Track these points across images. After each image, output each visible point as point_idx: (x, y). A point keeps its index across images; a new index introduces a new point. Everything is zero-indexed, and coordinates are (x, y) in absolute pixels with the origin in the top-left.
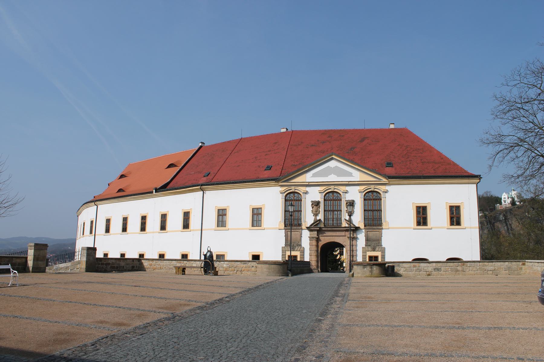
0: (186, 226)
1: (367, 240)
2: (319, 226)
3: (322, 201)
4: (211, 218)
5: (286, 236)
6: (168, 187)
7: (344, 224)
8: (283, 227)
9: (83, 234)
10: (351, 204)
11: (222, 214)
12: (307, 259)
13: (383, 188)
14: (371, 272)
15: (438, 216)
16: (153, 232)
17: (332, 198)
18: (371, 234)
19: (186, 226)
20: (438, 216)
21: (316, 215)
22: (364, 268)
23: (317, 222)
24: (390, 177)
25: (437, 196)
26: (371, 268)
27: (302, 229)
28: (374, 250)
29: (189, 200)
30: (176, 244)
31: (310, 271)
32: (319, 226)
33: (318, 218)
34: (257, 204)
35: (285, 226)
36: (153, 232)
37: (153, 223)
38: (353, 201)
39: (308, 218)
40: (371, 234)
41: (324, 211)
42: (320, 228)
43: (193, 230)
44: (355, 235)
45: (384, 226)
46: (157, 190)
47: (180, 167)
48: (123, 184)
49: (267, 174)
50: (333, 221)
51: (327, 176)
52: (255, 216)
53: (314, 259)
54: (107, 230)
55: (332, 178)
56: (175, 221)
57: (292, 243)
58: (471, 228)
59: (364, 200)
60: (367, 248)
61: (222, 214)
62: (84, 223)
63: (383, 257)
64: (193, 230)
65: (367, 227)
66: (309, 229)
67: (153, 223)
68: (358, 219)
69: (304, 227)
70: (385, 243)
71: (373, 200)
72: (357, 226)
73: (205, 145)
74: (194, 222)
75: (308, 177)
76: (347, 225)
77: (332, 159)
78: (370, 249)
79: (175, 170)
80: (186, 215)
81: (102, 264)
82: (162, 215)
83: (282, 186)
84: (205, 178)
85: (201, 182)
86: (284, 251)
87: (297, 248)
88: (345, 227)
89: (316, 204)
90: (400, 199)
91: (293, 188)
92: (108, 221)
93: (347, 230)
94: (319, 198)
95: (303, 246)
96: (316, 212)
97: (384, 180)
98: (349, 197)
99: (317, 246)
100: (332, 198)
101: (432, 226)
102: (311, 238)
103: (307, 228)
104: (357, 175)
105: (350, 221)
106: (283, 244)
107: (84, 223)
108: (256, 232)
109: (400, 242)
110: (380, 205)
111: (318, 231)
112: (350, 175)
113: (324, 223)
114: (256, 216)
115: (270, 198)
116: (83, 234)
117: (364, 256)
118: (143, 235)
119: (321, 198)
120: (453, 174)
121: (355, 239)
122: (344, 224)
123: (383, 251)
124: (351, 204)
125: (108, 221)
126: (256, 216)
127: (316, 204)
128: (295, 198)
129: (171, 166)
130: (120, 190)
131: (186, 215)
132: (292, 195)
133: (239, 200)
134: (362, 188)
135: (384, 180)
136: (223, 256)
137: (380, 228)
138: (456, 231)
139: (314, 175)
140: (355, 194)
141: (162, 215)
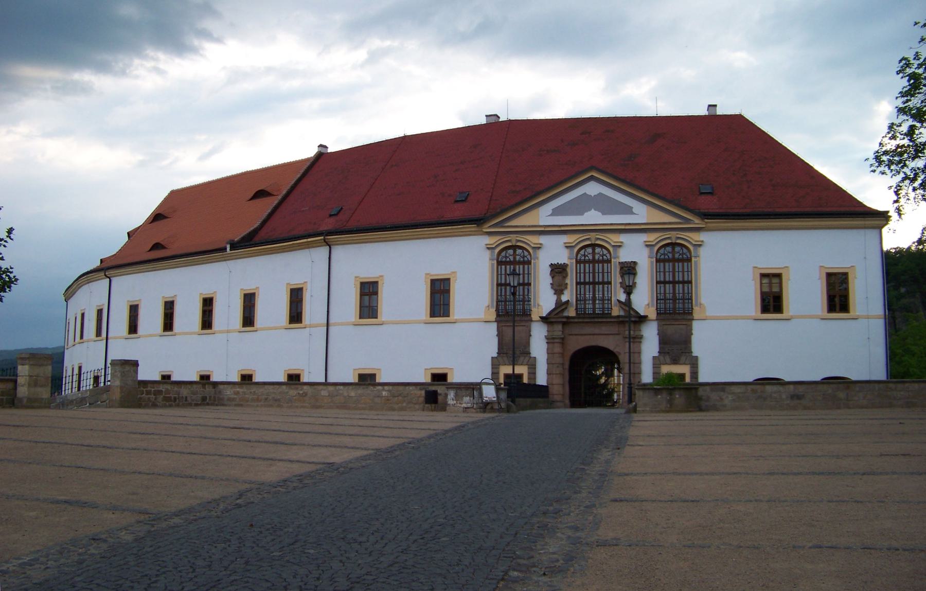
0: (296, 316)
1: (664, 341)
2: (566, 314)
3: (571, 263)
4: (347, 301)
5: (500, 335)
6: (257, 239)
7: (616, 311)
8: (493, 317)
9: (82, 337)
10: (629, 269)
11: (369, 292)
12: (542, 379)
13: (695, 237)
14: (671, 402)
15: (804, 294)
16: (228, 332)
17: (593, 256)
18: (670, 330)
19: (296, 316)
20: (804, 294)
21: (558, 290)
22: (656, 394)
23: (561, 306)
24: (705, 216)
25: (803, 254)
26: (671, 394)
27: (532, 321)
28: (675, 361)
29: (301, 266)
30: (272, 353)
31: (551, 405)
32: (566, 314)
33: (564, 298)
34: (440, 272)
35: (498, 315)
36: (228, 332)
37: (228, 313)
38: (635, 263)
39: (544, 299)
40: (670, 330)
41: (577, 283)
42: (568, 317)
43: (311, 326)
44: (637, 333)
45: (695, 315)
46: (234, 246)
47: (280, 197)
48: (161, 233)
49: (459, 211)
50: (594, 304)
51: (581, 213)
52: (437, 296)
53: (557, 380)
54: (133, 328)
55: (593, 217)
56: (272, 308)
57: (512, 348)
58: (868, 317)
59: (658, 261)
60: (662, 358)
61: (369, 292)
62: (83, 315)
63: (694, 374)
64: (311, 326)
65: (662, 316)
67: (228, 313)
68: (643, 299)
69: (535, 316)
70: (698, 347)
71: (675, 261)
72: (642, 314)
73: (329, 151)
74: (313, 309)
75: (544, 216)
76: (622, 313)
77: (592, 178)
78: (668, 360)
79: (267, 205)
80: (296, 296)
81: (148, 393)
82: (245, 295)
83: (490, 234)
84: (332, 220)
85: (324, 228)
86: (495, 364)
87: (522, 359)
88: (618, 317)
89: (558, 270)
90: (728, 260)
91: (513, 237)
92: (134, 310)
93: (620, 321)
95: (533, 355)
96: (560, 285)
97: (697, 222)
98: (625, 256)
99: (562, 355)
100: (593, 256)
101: (791, 314)
102: (550, 340)
104: (641, 213)
105: (628, 304)
106: (494, 351)
107: (83, 315)
108: (440, 330)
109: (729, 345)
110: (689, 271)
111: (564, 324)
112: (628, 210)
113: (576, 309)
114: (440, 296)
115: (466, 260)
116: (82, 337)
118: (207, 339)
119: (570, 258)
120: (834, 209)
121: (638, 339)
122: (616, 311)
123: (694, 363)
124: (629, 269)
125: (134, 310)
126: (440, 296)
127: (558, 270)
128: (518, 258)
129: (261, 194)
130: (157, 246)
131: (296, 296)
132: (511, 252)
133: (403, 264)
134: (652, 237)
135: (697, 221)
136: (373, 376)
137: (689, 317)
138: (838, 325)
139: (556, 212)
140: (635, 250)
141: (245, 295)
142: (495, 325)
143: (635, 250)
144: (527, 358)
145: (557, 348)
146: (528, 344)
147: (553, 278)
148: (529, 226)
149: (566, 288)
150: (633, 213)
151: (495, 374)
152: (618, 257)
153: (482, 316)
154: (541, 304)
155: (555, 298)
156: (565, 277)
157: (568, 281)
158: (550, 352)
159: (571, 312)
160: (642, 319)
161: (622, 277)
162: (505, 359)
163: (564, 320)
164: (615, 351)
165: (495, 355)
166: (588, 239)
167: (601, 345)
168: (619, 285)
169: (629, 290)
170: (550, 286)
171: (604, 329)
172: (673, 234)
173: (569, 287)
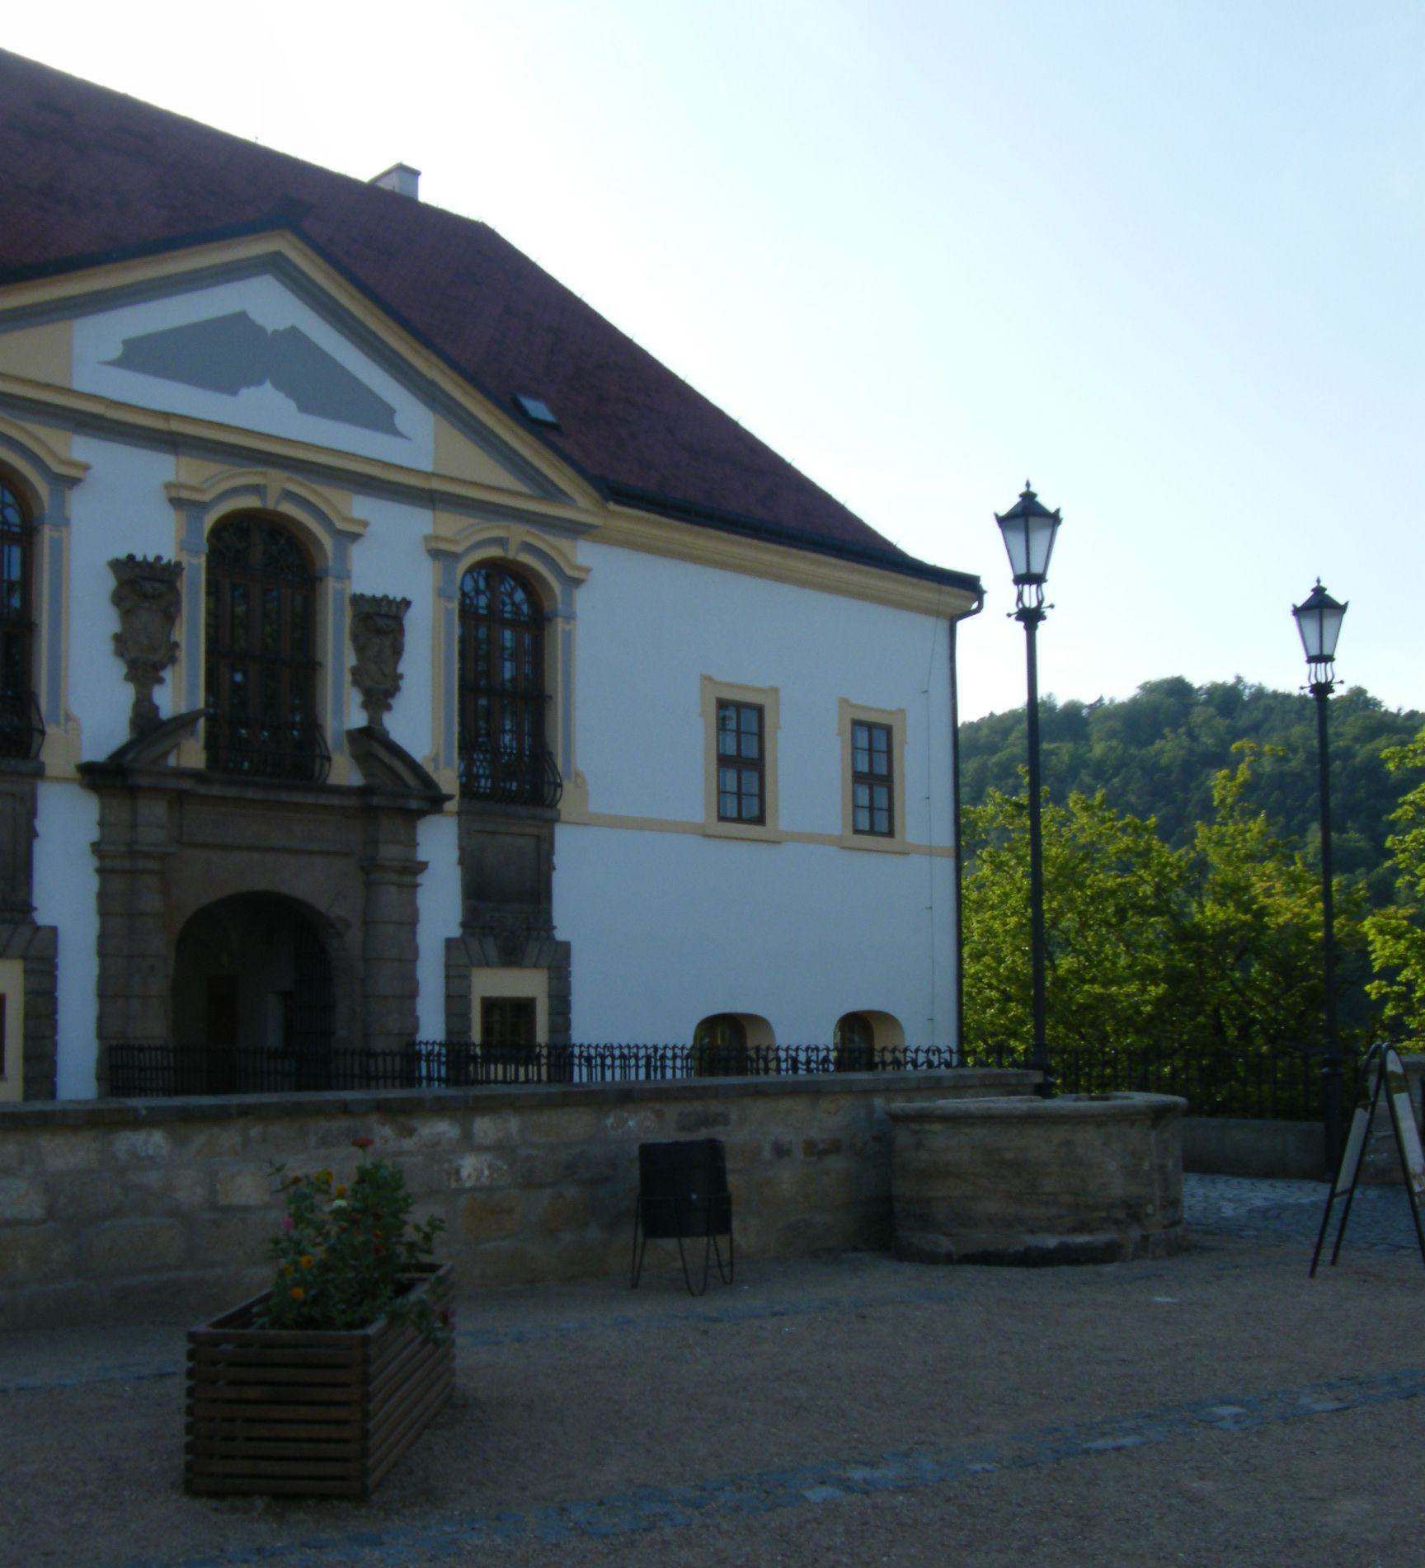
10: (380, 622)
21: (143, 662)
24: (615, 492)
28: (512, 957)
51: (229, 386)
55: (264, 411)
66: (95, 776)
77: (276, 265)
78: (491, 947)
89: (141, 586)
94: (160, 537)
95: (43, 917)
102: (116, 862)
104: (417, 439)
105: (371, 743)
112: (381, 418)
117: (456, 1003)
119: (182, 546)
123: (558, 962)
124: (380, 622)
127: (141, 586)
135: (582, 502)
139: (140, 355)
143: (391, 558)
145: (152, 902)
148: (48, 386)
149: (173, 660)
150: (396, 433)
152: (345, 575)
154: (76, 711)
155: (126, 695)
156: (170, 617)
157: (180, 634)
159: (192, 754)
161: (360, 650)
166: (257, 489)
167: (285, 890)
168: (348, 678)
169: (380, 691)
170: (108, 646)
172: (519, 533)
173: (182, 654)
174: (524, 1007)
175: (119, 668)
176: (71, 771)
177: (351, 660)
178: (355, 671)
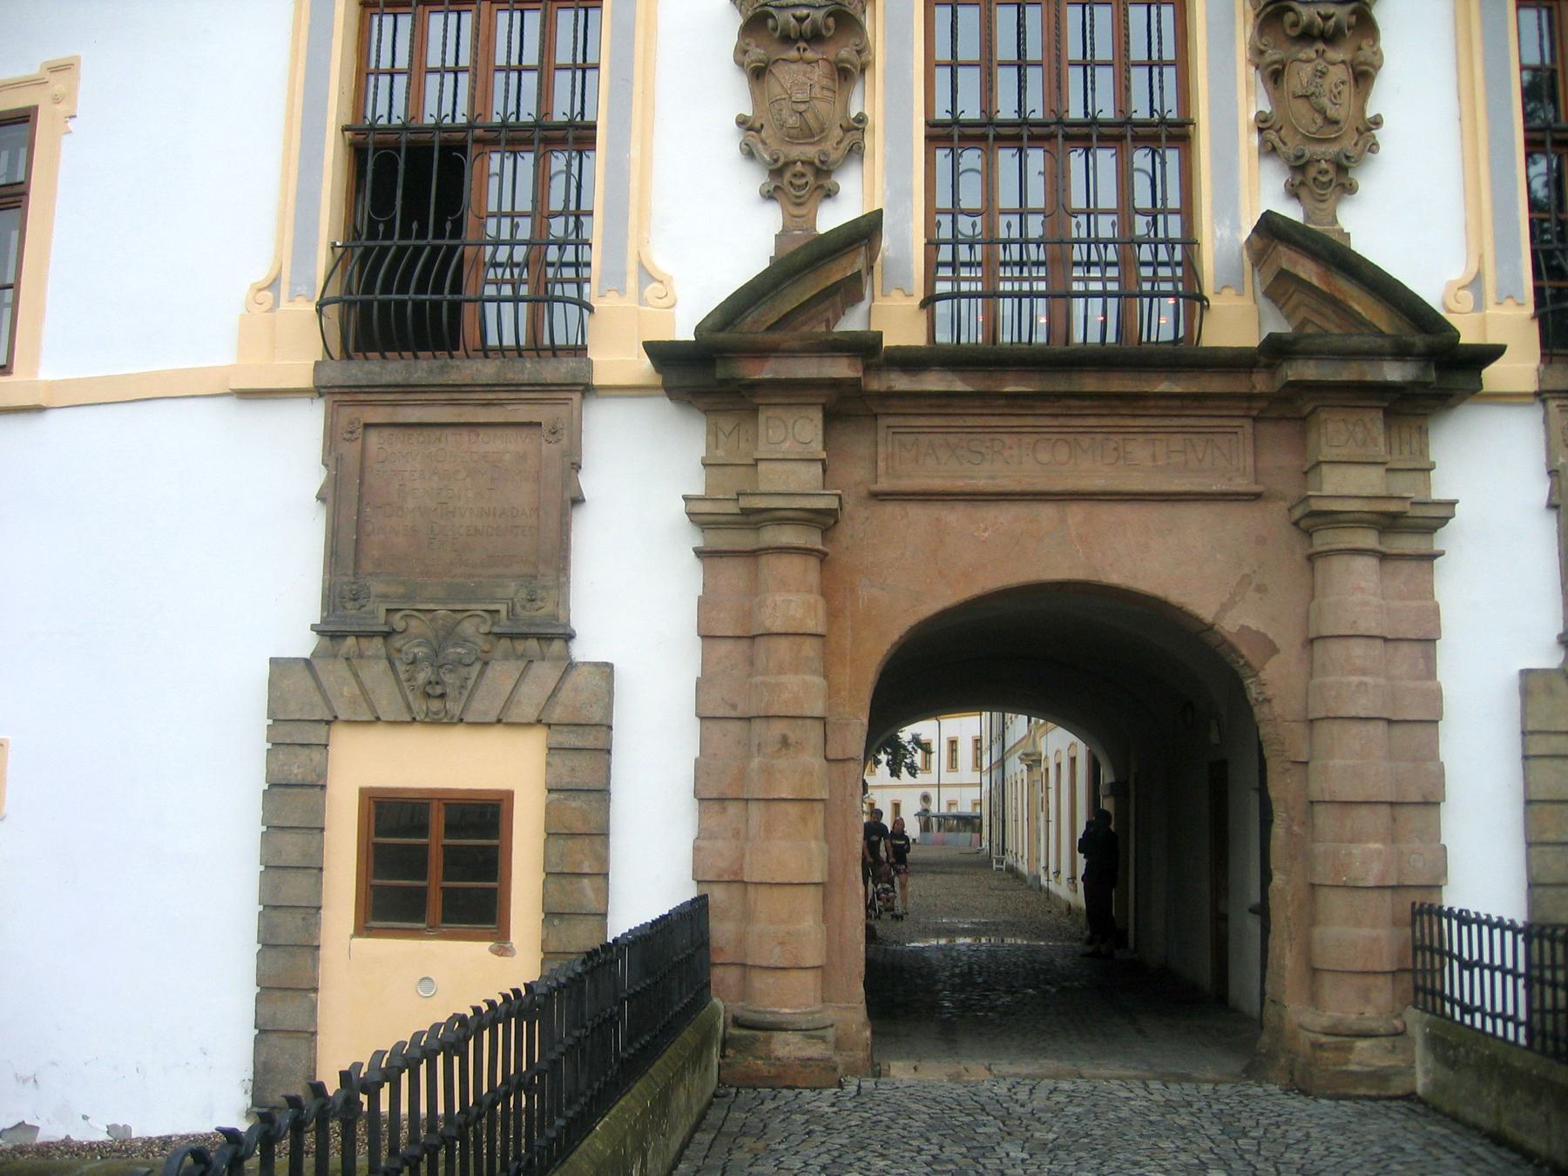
2: (852, 323)
5: (349, 499)
23: (819, 269)
27: (587, 389)
69: (617, 356)
76: (1278, 325)
87: (502, 674)
93: (1275, 393)
103: (662, 354)
121: (1408, 530)
122: (1236, 320)
142: (305, 426)
144: (545, 674)
146: (552, 560)
147: (758, 74)
149: (855, 151)
151: (291, 798)
153: (217, 349)
154: (660, 261)
156: (846, 75)
158: (730, 636)
160: (1448, 369)
162: (375, 671)
163: (841, 368)
164: (1229, 625)
165: (302, 644)
167: (1114, 578)
170: (729, 141)
171: (1145, 460)
173: (876, 142)
174: (482, 817)
175: (752, 179)
176: (640, 368)
177: (1252, 101)
178: (1263, 125)
